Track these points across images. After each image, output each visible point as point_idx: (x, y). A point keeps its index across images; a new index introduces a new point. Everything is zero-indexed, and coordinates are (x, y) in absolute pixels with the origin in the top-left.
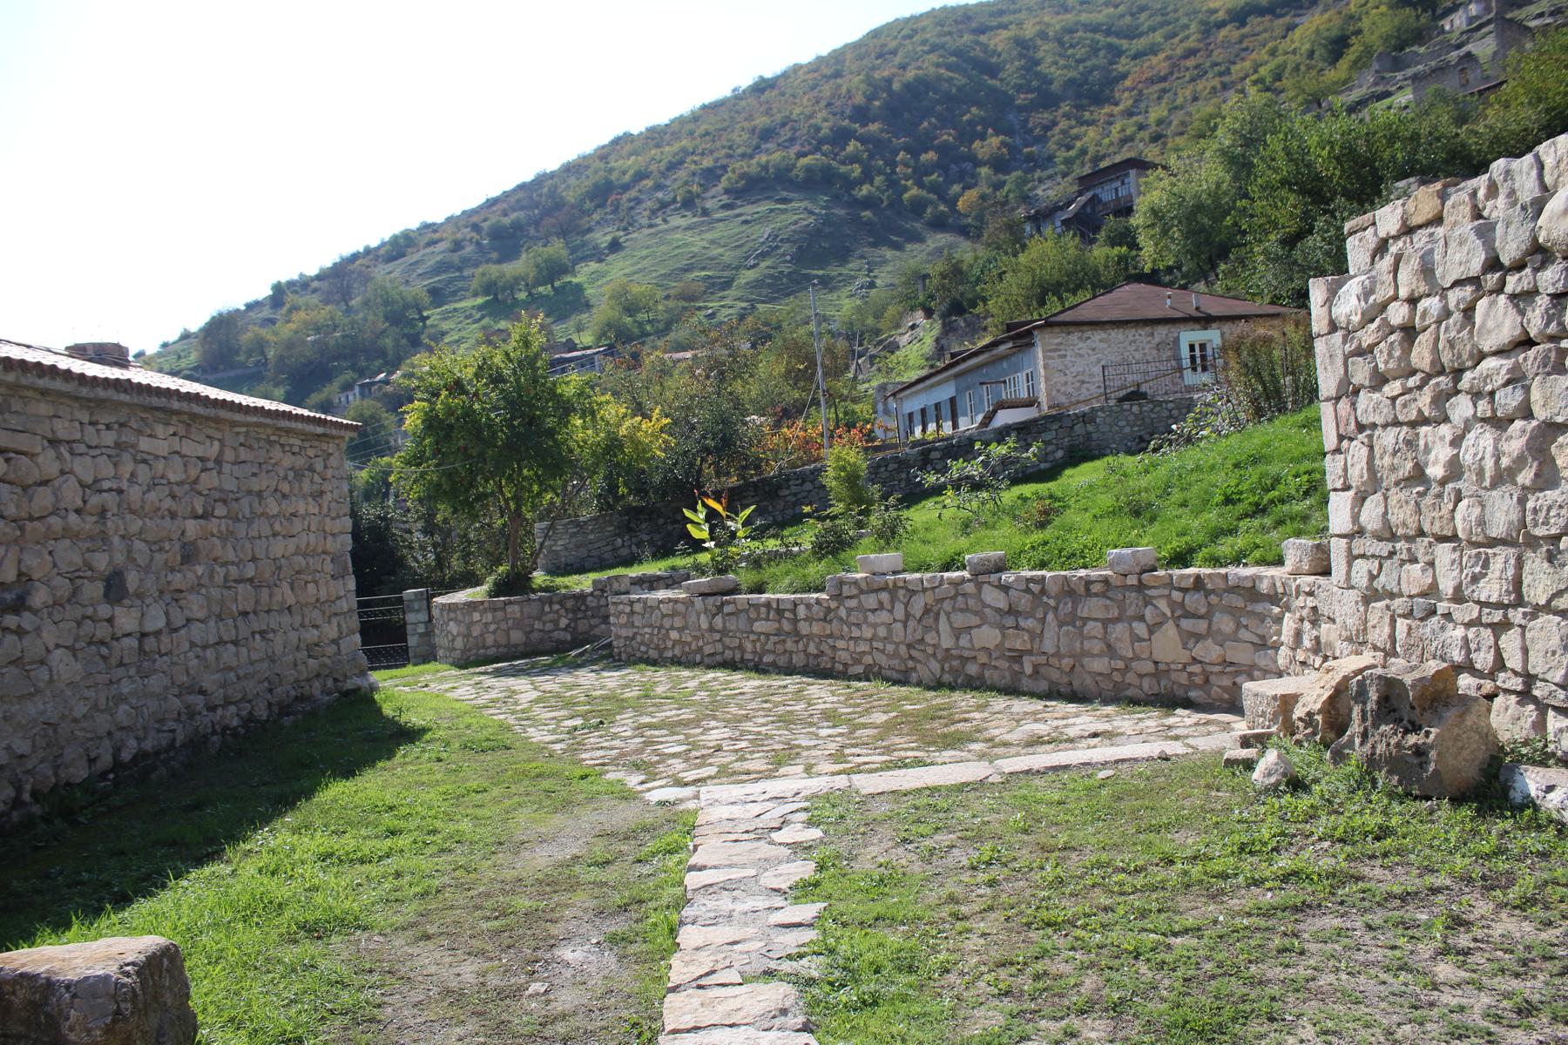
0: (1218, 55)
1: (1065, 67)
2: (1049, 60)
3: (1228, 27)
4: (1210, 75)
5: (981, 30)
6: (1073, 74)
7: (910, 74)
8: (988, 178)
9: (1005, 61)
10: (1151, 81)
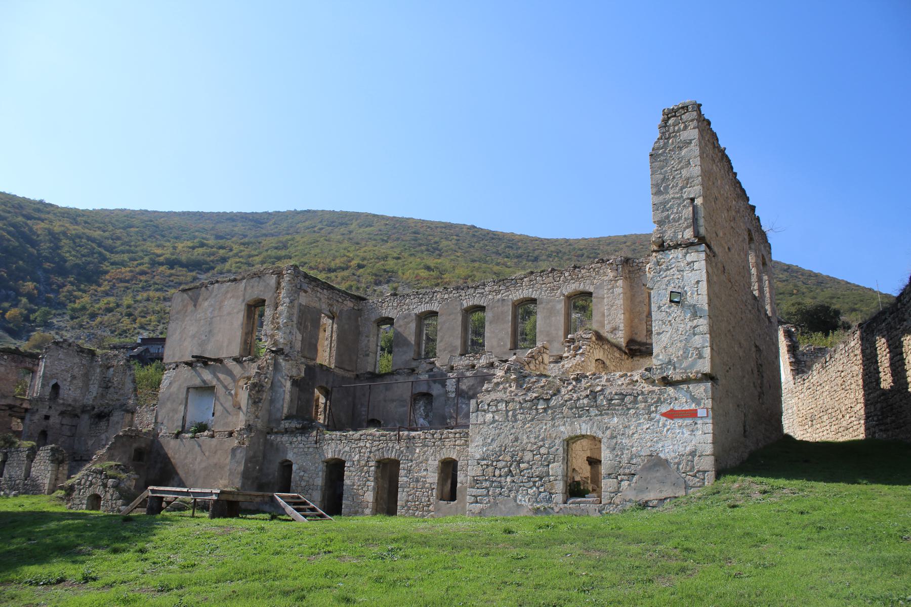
0: (157, 279)
1: (74, 256)
3: (165, 267)
4: (152, 288)
5: (29, 217)
6: (78, 261)
8: (25, 304)
9: (41, 241)
10: (122, 281)
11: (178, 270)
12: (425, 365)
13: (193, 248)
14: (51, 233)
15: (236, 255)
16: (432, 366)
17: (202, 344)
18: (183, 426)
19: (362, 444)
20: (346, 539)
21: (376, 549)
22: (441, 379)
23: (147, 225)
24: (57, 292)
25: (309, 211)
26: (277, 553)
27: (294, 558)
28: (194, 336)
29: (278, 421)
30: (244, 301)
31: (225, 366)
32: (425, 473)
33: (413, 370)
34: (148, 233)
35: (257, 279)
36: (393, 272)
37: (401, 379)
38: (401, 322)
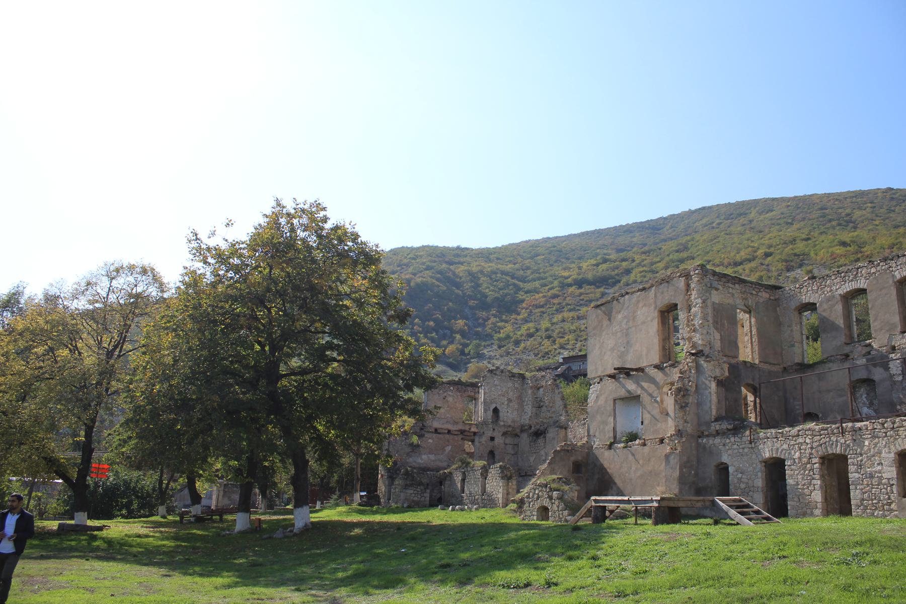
1: (493, 291)
2: (485, 285)
4: (566, 309)
5: (450, 263)
6: (497, 295)
7: (419, 280)
10: (537, 307)
11: (586, 288)
12: (860, 348)
13: (597, 265)
14: (470, 273)
15: (639, 265)
16: (868, 349)
17: (622, 356)
18: (615, 437)
19: (801, 440)
20: (800, 542)
21: (837, 554)
22: (883, 362)
23: (552, 251)
24: (483, 325)
25: (704, 208)
26: (728, 559)
27: (747, 563)
28: (612, 350)
29: (708, 424)
30: (656, 308)
31: (647, 375)
32: (879, 468)
33: (847, 356)
34: (554, 258)
35: (666, 284)
36: (804, 254)
37: (834, 366)
38: (825, 306)
